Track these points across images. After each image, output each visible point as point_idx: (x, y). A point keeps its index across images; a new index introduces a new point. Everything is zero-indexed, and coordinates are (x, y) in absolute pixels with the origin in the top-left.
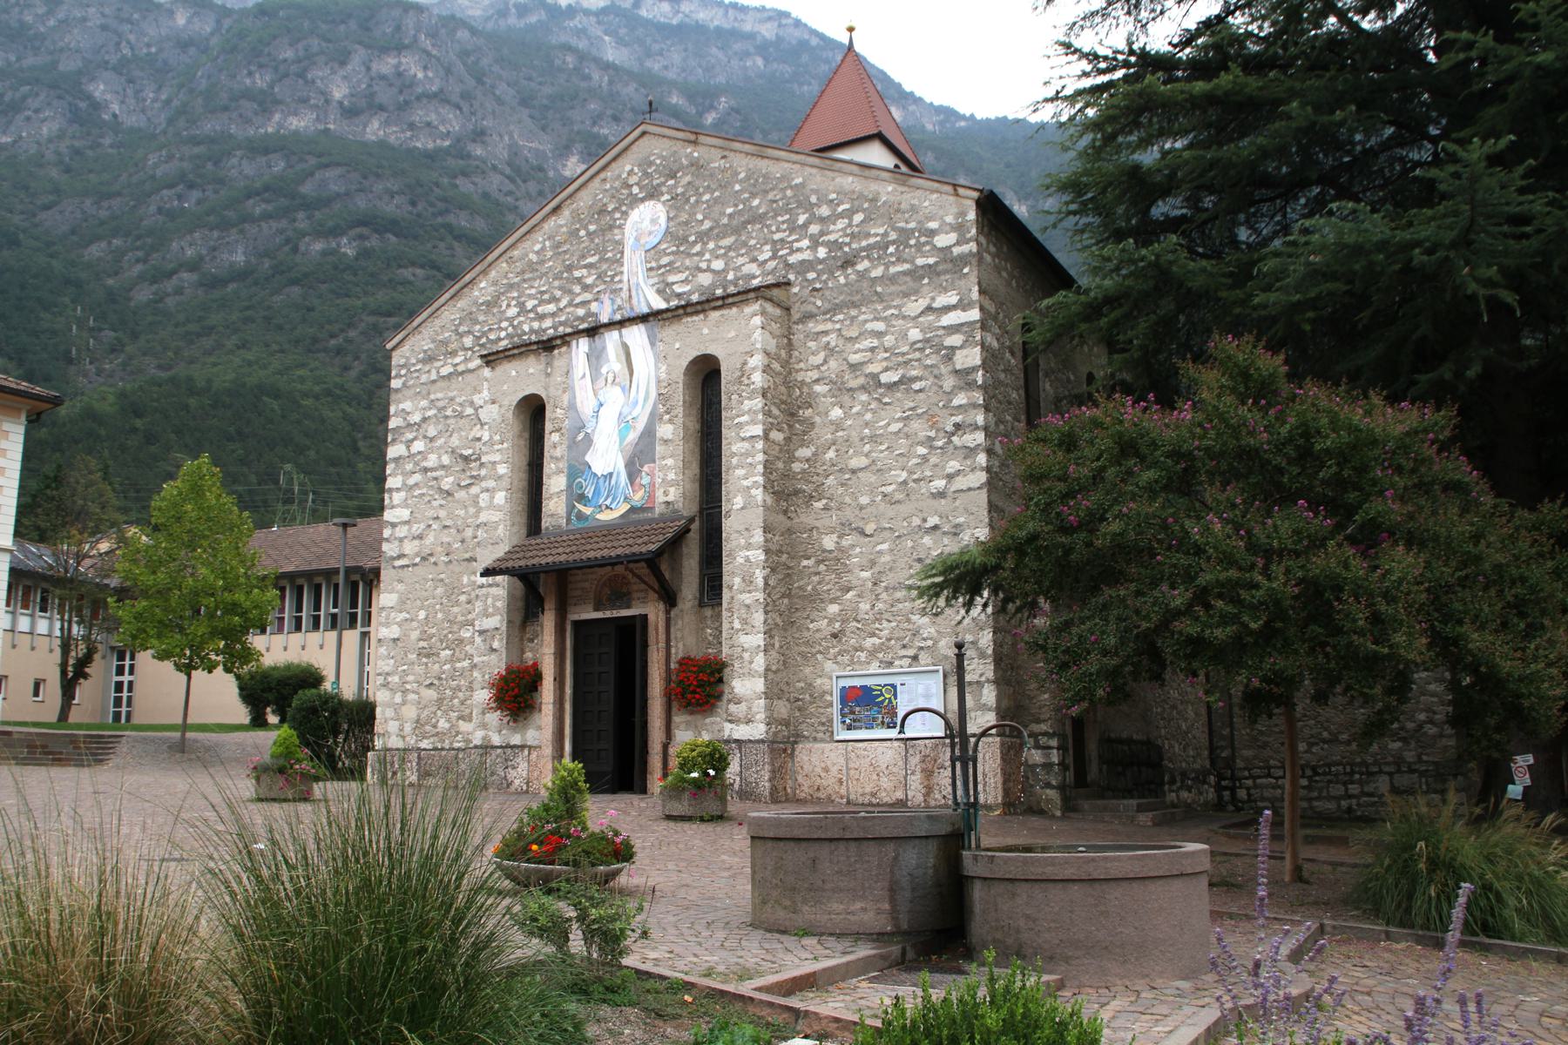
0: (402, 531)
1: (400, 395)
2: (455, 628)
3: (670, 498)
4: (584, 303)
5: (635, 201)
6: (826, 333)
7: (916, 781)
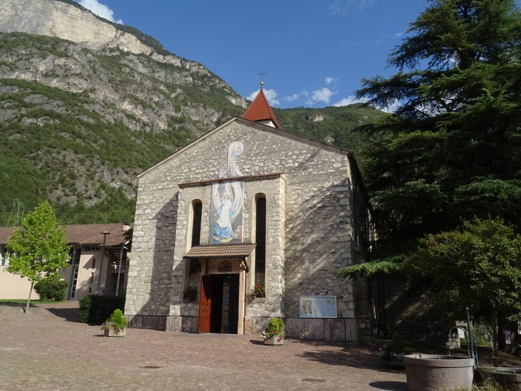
0: (140, 239)
1: (141, 194)
4: (213, 171)
5: (232, 141)
6: (298, 189)
7: (327, 332)
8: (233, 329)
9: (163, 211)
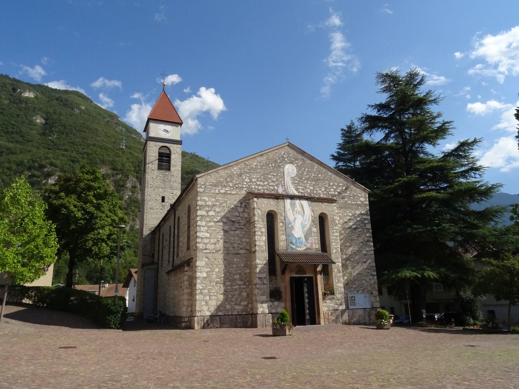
0: (206, 241)
1: (202, 194)
2: (232, 275)
3: (317, 247)
4: (272, 186)
5: (286, 163)
7: (367, 318)
8: (314, 320)
9: (228, 215)
